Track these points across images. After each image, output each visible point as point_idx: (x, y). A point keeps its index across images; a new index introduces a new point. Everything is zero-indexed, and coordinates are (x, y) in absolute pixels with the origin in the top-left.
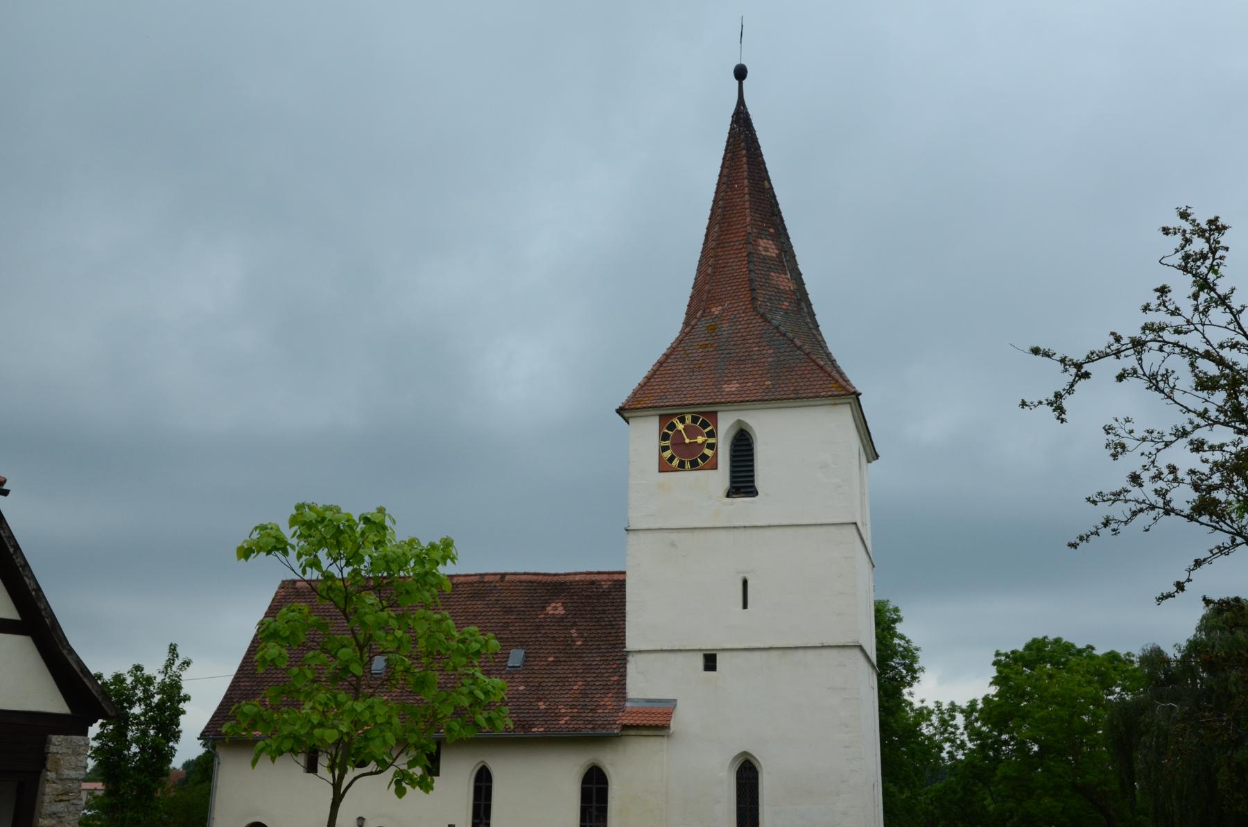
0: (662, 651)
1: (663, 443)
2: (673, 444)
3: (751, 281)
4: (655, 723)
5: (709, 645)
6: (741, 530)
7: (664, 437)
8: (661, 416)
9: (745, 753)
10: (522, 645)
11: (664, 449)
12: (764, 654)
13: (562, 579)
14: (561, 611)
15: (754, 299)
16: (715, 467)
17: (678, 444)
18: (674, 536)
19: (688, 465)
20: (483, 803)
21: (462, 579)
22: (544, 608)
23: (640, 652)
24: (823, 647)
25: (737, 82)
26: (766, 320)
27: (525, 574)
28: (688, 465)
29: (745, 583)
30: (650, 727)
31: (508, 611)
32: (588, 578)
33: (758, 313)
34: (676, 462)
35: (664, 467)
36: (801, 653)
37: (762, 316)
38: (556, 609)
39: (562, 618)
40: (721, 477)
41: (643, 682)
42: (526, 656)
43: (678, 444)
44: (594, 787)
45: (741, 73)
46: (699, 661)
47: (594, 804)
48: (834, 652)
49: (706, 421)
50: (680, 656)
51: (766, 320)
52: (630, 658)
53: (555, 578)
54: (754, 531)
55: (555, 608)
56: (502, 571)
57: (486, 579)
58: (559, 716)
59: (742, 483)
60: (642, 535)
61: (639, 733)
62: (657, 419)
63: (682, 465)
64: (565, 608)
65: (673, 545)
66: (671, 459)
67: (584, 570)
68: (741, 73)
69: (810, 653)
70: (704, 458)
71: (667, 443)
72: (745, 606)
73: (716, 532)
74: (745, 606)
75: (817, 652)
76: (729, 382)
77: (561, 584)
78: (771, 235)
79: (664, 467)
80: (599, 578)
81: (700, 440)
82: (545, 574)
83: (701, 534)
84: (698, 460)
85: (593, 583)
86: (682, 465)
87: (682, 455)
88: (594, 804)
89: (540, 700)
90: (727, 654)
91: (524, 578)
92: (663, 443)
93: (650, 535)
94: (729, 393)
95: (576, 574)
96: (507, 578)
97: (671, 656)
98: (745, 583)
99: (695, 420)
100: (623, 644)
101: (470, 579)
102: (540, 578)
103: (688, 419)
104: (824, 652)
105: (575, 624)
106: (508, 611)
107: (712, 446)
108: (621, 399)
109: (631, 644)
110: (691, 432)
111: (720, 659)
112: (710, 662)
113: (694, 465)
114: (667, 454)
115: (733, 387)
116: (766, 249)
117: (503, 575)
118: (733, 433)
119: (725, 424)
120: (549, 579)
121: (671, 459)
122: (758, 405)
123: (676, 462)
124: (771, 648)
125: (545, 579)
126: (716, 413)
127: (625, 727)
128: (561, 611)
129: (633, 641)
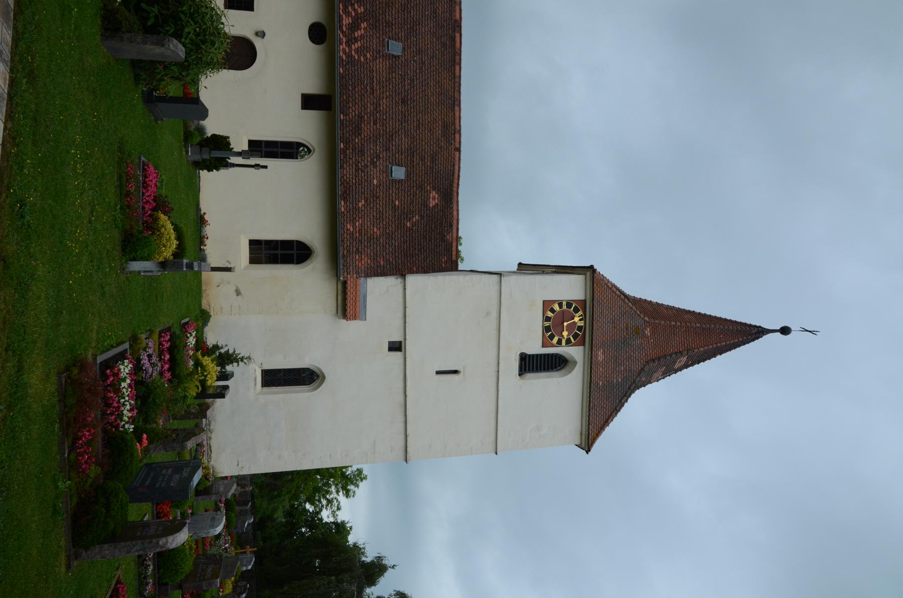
0: (405, 308)
1: (564, 303)
2: (563, 312)
3: (665, 356)
4: (347, 306)
5: (409, 347)
6: (495, 369)
7: (569, 305)
8: (585, 301)
9: (324, 378)
10: (408, 174)
12: (401, 390)
13: (454, 201)
14: (432, 203)
15: (653, 361)
16: (544, 345)
17: (564, 316)
18: (494, 314)
19: (547, 324)
20: (280, 150)
21: (457, 114)
22: (434, 188)
23: (405, 289)
24: (406, 436)
27: (459, 168)
28: (547, 324)
30: (344, 299)
31: (433, 159)
32: (455, 222)
33: (645, 366)
34: (550, 314)
35: (547, 305)
36: (403, 419)
37: (642, 369)
38: (434, 199)
39: (425, 205)
40: (535, 347)
41: (379, 291)
42: (400, 181)
43: (564, 316)
44: (294, 252)
45: (785, 331)
46: (397, 338)
47: (279, 252)
48: (402, 443)
49: (578, 338)
50: (401, 322)
52: (400, 280)
53: (455, 194)
54: (495, 379)
55: (434, 198)
57: (457, 136)
59: (530, 364)
60: (496, 287)
61: (340, 292)
62: (583, 298)
63: (547, 319)
64: (434, 207)
65: (488, 314)
66: (552, 311)
68: (785, 331)
69: (402, 425)
71: (565, 307)
72: (438, 373)
73: (495, 349)
74: (438, 373)
75: (403, 431)
76: (604, 353)
79: (547, 305)
80: (454, 230)
81: (565, 333)
82: (458, 184)
84: (550, 331)
85: (451, 226)
86: (547, 319)
87: (555, 318)
88: (279, 252)
90: (401, 361)
91: (457, 168)
92: (564, 303)
93: (495, 295)
95: (458, 210)
96: (457, 153)
99: (580, 328)
100: (412, 272)
102: (456, 181)
103: (581, 324)
104: (402, 436)
106: (433, 159)
107: (559, 342)
108: (599, 268)
109: (411, 279)
111: (398, 355)
112: (396, 347)
113: (547, 329)
114: (556, 307)
115: (601, 357)
117: (459, 150)
118: (567, 356)
119: (575, 352)
120: (455, 189)
121: (552, 311)
122: (587, 378)
123: (550, 314)
124: (406, 396)
125: (455, 185)
126: (584, 344)
127: (345, 283)
128: (432, 203)
129: (414, 281)
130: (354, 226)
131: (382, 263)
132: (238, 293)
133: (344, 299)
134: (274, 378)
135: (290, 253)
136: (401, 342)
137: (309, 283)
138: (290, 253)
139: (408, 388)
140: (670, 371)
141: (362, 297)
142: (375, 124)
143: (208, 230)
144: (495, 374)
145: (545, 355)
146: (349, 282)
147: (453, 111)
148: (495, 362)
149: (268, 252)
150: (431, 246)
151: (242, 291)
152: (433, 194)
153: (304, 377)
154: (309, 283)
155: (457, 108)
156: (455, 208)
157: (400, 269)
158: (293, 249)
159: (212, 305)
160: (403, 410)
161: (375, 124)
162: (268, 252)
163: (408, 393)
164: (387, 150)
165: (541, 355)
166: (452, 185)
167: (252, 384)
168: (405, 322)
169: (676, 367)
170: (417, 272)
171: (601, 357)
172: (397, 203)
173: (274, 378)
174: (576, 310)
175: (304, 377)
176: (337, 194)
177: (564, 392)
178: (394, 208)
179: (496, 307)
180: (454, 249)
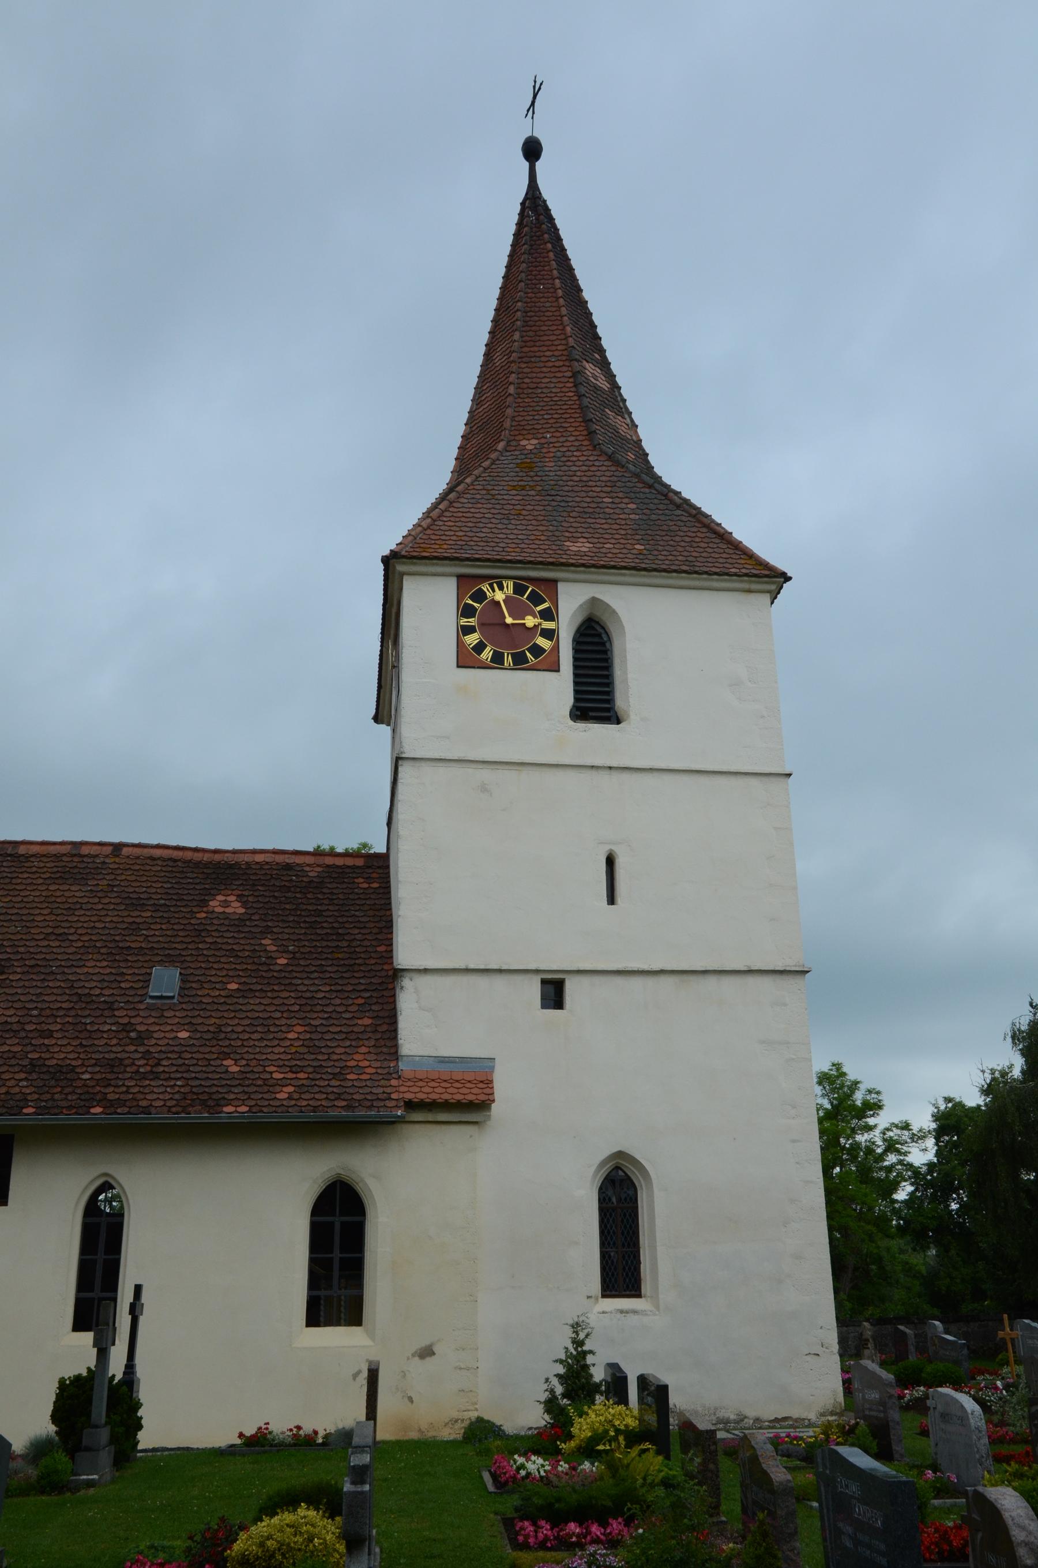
0: (467, 971)
1: (464, 621)
2: (482, 625)
4: (462, 1099)
5: (553, 962)
6: (604, 777)
7: (467, 611)
8: (460, 577)
9: (620, 1154)
10: (169, 960)
11: (467, 630)
12: (650, 982)
13: (227, 858)
14: (236, 908)
15: (591, 433)
16: (555, 667)
17: (493, 623)
18: (485, 774)
19: (508, 660)
20: (101, 1256)
21: (35, 849)
22: (204, 903)
23: (426, 971)
24: (750, 972)
25: (527, 164)
26: (617, 464)
27: (158, 846)
28: (508, 660)
29: (610, 861)
30: (447, 1106)
32: (279, 859)
33: (603, 453)
34: (487, 654)
35: (466, 659)
36: (711, 981)
37: (610, 458)
39: (241, 921)
40: (559, 688)
41: (429, 1028)
43: (493, 623)
44: (337, 1220)
45: (532, 150)
46: (533, 990)
47: (337, 1255)
48: (767, 982)
49: (540, 593)
51: (617, 464)
52: (406, 982)
53: (217, 857)
54: (626, 776)
55: (226, 904)
56: (116, 839)
57: (85, 850)
58: (271, 1085)
60: (426, 768)
61: (430, 1117)
63: (497, 659)
64: (244, 904)
65: (484, 788)
66: (480, 648)
67: (270, 847)
68: (532, 150)
70: (537, 651)
71: (472, 621)
72: (611, 900)
73: (560, 774)
74: (611, 900)
76: (574, 539)
77: (230, 866)
78: (596, 360)
79: (466, 659)
80: (299, 860)
81: (530, 621)
82: (196, 850)
83: (535, 775)
84: (525, 655)
85: (288, 867)
86: (497, 659)
87: (496, 643)
88: (337, 1255)
89: (226, 1056)
90: (585, 981)
91: (158, 853)
92: (464, 621)
94: (577, 553)
95: (254, 852)
96: (125, 851)
97: (482, 981)
98: (610, 861)
99: (519, 590)
100: (388, 955)
101: (52, 849)
102: (189, 855)
103: (509, 586)
104: (751, 981)
105: (266, 931)
107: (549, 634)
108: (390, 543)
109: (405, 955)
110: (518, 611)
111: (572, 989)
112: (554, 993)
113: (520, 661)
114: (472, 639)
116: (596, 378)
119: (572, 601)
120: (206, 857)
121: (480, 648)
122: (629, 576)
123: (487, 654)
124: (662, 972)
125: (197, 857)
126: (554, 582)
127: (411, 1106)
128: (236, 908)
129: (407, 950)
130: (282, 1084)
131: (367, 1021)
132: (427, 1352)
133: (447, 1106)
134: (622, 1271)
135: (339, 1233)
136: (544, 982)
137: (408, 1184)
138: (339, 1233)
139: (646, 967)
140: (613, 399)
141: (442, 1067)
142: (50, 1034)
143: (280, 1426)
144: (616, 777)
145: (576, 667)
146: (409, 1096)
147: (28, 857)
148: (587, 775)
149: (336, 1285)
150: (329, 913)
151: (424, 1343)
152: (215, 904)
153: (620, 1196)
154: (408, 1184)
155: (22, 850)
156: (247, 858)
157: (377, 981)
158: (332, 1224)
159: (455, 1414)
160: (692, 978)
161: (50, 1034)
162: (336, 1285)
163: (656, 967)
164: (111, 1006)
165: (576, 675)
166: (198, 864)
167: (633, 1319)
168: (500, 971)
169: (605, 385)
170: (389, 943)
171: (581, 546)
172: (233, 986)
173: (622, 1271)
174: (479, 596)
175: (620, 1196)
176: (206, 1123)
177: (657, 627)
178: (244, 992)
179: (470, 770)
180: (339, 862)
